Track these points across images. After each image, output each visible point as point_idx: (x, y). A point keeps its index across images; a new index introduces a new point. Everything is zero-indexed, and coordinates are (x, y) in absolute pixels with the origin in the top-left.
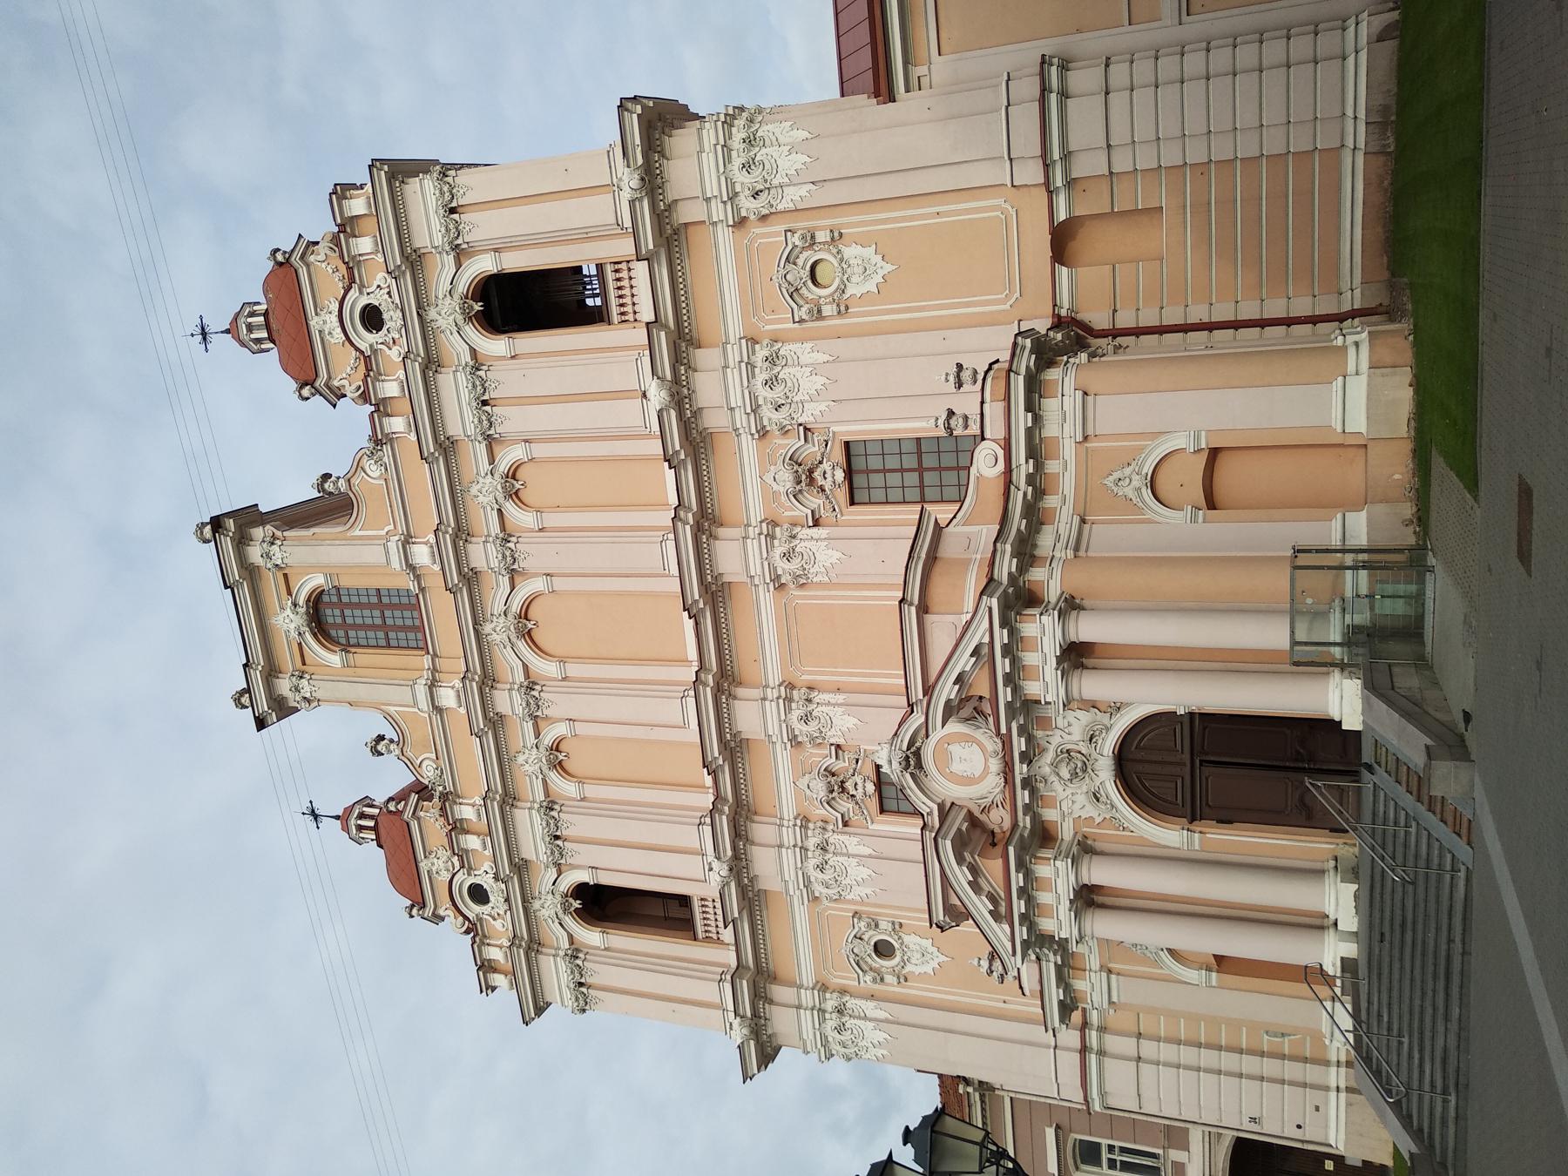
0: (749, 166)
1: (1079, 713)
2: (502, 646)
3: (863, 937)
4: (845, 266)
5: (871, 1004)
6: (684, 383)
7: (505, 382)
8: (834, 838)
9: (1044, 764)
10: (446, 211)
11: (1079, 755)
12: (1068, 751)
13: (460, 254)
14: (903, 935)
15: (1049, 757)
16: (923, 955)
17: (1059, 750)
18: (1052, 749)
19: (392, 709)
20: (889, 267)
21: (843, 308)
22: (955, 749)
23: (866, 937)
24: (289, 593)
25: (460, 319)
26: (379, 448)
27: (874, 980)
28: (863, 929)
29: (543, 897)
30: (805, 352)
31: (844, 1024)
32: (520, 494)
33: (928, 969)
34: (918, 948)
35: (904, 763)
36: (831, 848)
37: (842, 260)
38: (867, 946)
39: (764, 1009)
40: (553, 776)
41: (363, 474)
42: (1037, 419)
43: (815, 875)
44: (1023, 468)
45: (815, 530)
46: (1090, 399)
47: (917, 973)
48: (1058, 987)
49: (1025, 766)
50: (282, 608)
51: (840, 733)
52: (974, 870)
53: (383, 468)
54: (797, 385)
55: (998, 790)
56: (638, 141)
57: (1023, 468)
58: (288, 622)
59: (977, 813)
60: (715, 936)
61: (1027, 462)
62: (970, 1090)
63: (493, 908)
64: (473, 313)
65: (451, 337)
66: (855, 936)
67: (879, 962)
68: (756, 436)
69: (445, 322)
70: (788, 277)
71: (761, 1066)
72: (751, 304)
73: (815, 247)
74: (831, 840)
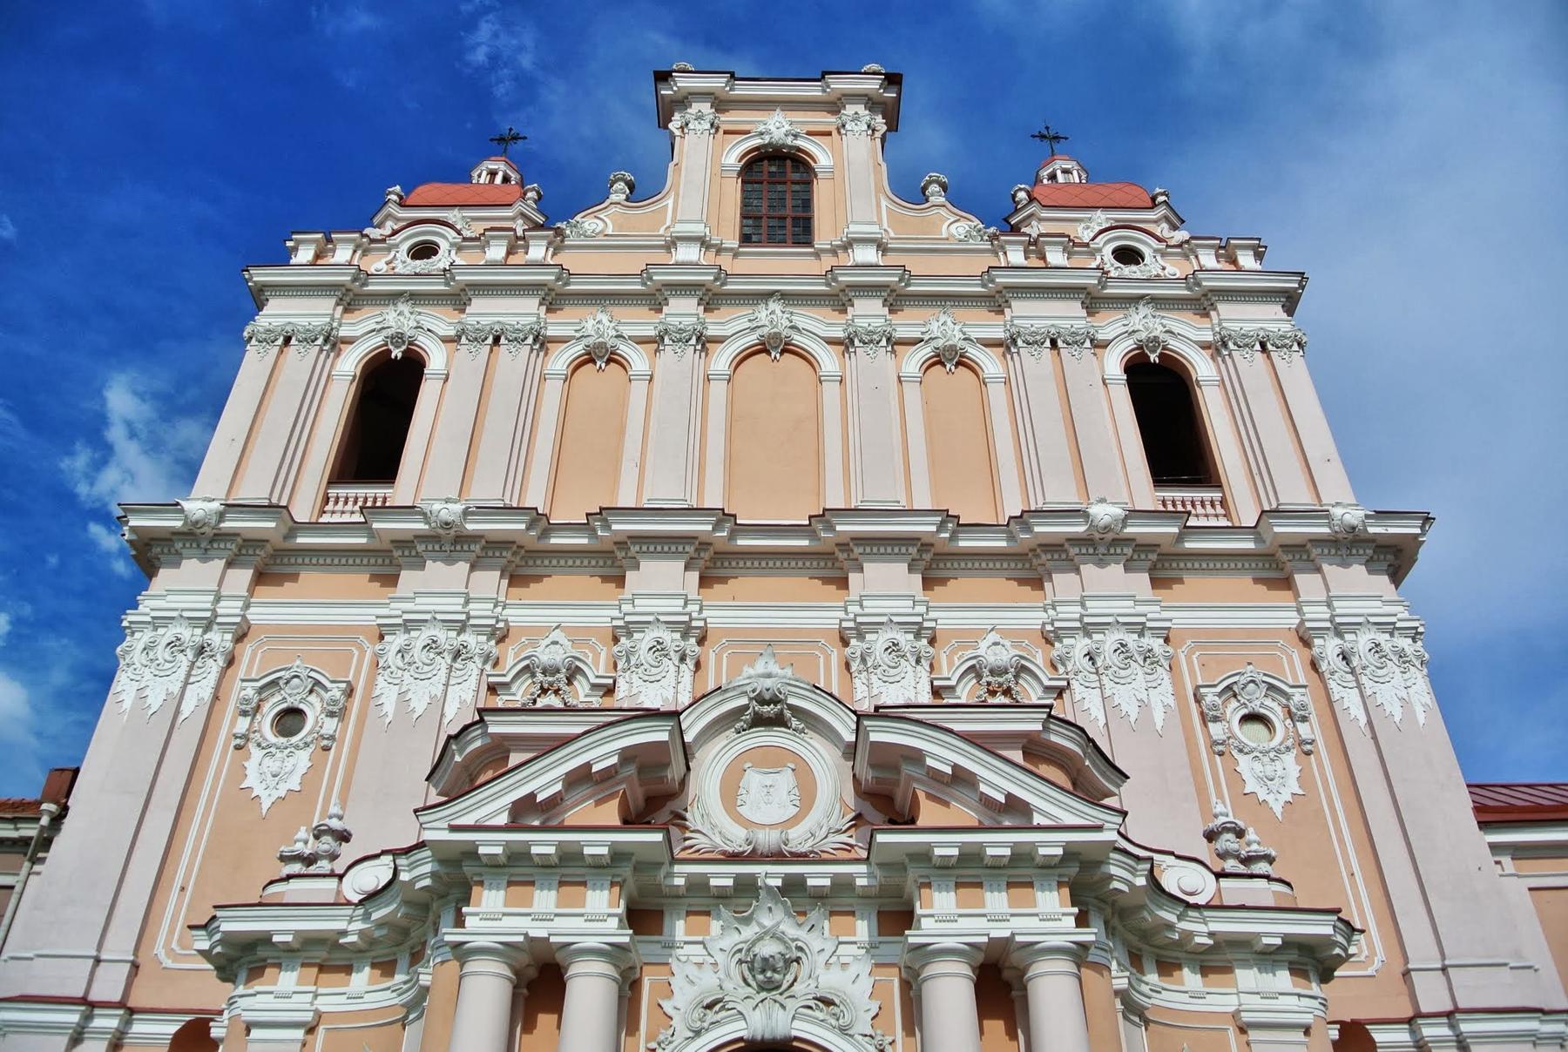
0: (1377, 652)
1: (866, 984)
3: (314, 695)
4: (1272, 754)
5: (207, 694)
6: (1112, 551)
7: (1078, 362)
8: (474, 668)
9: (771, 917)
10: (1263, 338)
11: (790, 978)
12: (798, 960)
13: (1217, 348)
14: (310, 750)
15: (789, 929)
16: (274, 776)
17: (800, 944)
18: (801, 933)
19: (670, 202)
20: (1278, 809)
21: (1221, 748)
22: (785, 781)
23: (312, 698)
24: (809, 133)
25: (1143, 336)
26: (986, 238)
27: (247, 701)
28: (327, 696)
29: (413, 317)
30: (1162, 697)
31: (182, 651)
32: (939, 367)
33: (252, 780)
34: (287, 770)
35: (767, 696)
36: (456, 665)
37: (1278, 751)
38: (298, 697)
40: (578, 349)
41: (952, 220)
42: (1267, 958)
43: (421, 637)
44: (1202, 928)
45: (928, 688)
46: (1299, 1036)
47: (246, 764)
48: (297, 933)
49: (779, 882)
50: (791, 123)
51: (635, 691)
52: (608, 775)
54: (1122, 681)
55: (718, 840)
56: (1392, 530)
57: (1202, 928)
58: (777, 127)
59: (674, 805)
60: (329, 507)
61: (1211, 935)
62: (45, 820)
63: (404, 262)
64: (1147, 351)
65: (1120, 324)
66: (317, 683)
67: (271, 709)
68: (1049, 628)
69: (1137, 321)
70: (1252, 685)
71: (136, 534)
72: (1207, 639)
73: (1289, 721)
74: (470, 665)
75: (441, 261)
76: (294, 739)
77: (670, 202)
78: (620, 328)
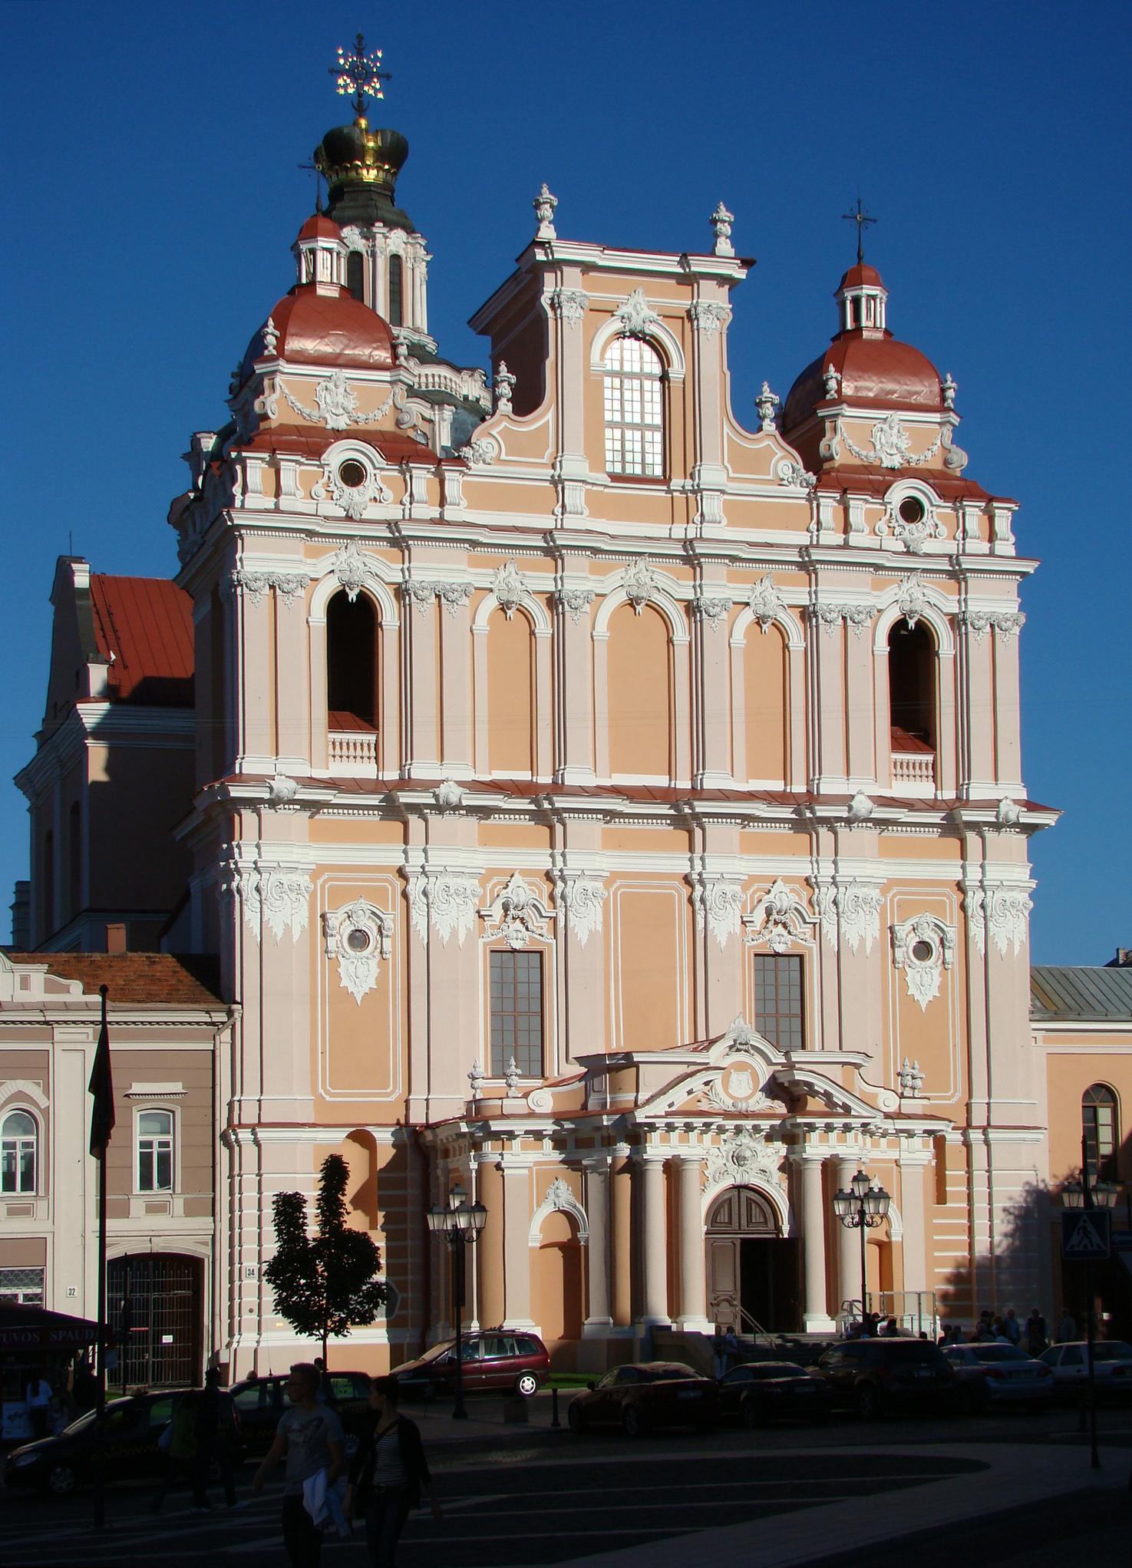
2: (623, 575)
5: (306, 924)
26: (805, 485)
39: (290, 809)
53: (785, 482)
75: (369, 487)
76: (366, 952)
77: (550, 417)
78: (524, 581)
